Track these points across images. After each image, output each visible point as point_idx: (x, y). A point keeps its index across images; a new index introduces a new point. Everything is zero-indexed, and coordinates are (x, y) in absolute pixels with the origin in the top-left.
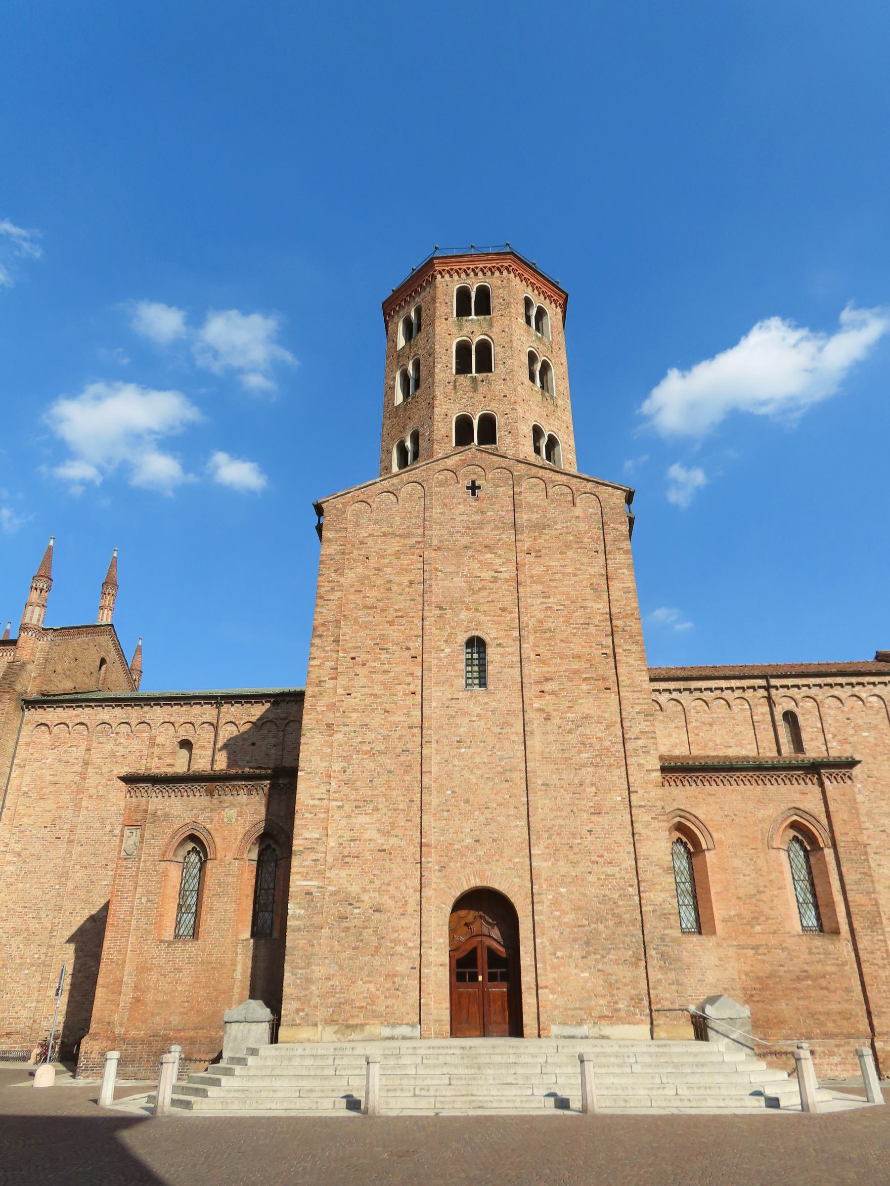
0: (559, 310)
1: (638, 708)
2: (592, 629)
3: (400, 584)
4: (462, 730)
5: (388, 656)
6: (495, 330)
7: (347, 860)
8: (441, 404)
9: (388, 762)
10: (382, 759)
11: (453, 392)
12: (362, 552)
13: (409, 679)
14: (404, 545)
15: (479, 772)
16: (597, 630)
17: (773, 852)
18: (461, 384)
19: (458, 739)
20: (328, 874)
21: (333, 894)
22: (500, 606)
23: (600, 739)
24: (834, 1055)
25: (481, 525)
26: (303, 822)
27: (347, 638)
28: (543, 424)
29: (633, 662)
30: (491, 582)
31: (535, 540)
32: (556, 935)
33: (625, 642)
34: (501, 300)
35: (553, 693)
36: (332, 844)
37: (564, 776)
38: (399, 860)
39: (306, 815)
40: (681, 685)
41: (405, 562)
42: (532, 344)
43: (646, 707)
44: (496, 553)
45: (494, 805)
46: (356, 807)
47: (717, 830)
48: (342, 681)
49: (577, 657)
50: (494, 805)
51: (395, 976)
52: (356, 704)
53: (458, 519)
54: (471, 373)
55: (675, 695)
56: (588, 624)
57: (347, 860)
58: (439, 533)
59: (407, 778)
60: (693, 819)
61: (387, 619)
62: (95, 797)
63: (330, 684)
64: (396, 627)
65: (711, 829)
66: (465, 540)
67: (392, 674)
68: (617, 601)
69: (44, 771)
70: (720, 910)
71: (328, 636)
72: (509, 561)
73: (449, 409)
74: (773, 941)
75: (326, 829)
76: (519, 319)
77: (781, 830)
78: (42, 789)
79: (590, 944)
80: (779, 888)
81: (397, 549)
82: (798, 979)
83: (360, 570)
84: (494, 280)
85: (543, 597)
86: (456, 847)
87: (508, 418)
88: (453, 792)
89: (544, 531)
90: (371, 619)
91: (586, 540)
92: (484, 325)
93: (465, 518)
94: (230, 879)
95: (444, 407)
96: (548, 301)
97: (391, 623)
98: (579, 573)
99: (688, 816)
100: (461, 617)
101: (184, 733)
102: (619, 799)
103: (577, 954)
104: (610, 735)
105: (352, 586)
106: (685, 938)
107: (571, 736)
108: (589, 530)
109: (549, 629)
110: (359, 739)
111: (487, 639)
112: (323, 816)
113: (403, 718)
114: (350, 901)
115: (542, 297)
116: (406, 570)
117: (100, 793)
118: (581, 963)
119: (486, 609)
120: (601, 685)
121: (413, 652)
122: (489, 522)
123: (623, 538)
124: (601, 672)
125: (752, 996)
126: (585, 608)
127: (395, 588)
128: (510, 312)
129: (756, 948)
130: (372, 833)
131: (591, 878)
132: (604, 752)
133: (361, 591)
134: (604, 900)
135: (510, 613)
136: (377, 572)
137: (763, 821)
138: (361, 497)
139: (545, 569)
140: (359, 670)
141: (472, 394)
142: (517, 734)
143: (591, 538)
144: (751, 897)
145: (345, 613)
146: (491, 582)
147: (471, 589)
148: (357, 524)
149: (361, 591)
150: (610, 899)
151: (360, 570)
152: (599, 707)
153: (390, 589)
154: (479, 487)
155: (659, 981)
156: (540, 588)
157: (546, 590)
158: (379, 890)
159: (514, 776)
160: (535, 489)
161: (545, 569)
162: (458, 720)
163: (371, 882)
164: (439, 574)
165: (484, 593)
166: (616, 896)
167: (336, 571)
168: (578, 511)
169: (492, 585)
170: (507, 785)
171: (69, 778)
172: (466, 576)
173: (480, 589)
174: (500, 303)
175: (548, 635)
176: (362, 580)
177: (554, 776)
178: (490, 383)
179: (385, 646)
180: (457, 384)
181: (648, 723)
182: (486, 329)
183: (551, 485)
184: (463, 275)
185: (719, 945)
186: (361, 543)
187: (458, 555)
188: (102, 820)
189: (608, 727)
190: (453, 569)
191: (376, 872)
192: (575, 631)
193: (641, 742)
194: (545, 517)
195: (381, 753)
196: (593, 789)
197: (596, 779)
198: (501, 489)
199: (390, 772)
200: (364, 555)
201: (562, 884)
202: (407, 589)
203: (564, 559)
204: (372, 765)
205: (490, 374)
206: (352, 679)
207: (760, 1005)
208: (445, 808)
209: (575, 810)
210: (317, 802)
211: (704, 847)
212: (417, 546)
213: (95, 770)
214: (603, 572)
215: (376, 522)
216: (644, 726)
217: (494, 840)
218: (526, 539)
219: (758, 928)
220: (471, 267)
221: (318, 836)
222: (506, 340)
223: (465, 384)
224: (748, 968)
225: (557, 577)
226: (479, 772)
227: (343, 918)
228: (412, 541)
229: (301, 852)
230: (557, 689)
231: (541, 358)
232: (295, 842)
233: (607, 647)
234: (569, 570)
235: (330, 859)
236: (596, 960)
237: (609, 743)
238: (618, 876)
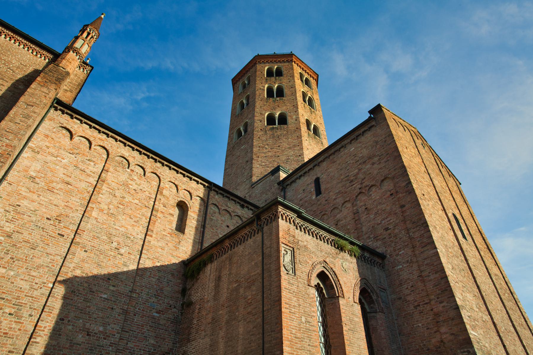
62: (105, 212)
69: (58, 167)
78: (52, 182)
101: (183, 196)
117: (111, 211)
171: (83, 185)
188: (110, 235)
213: (109, 190)
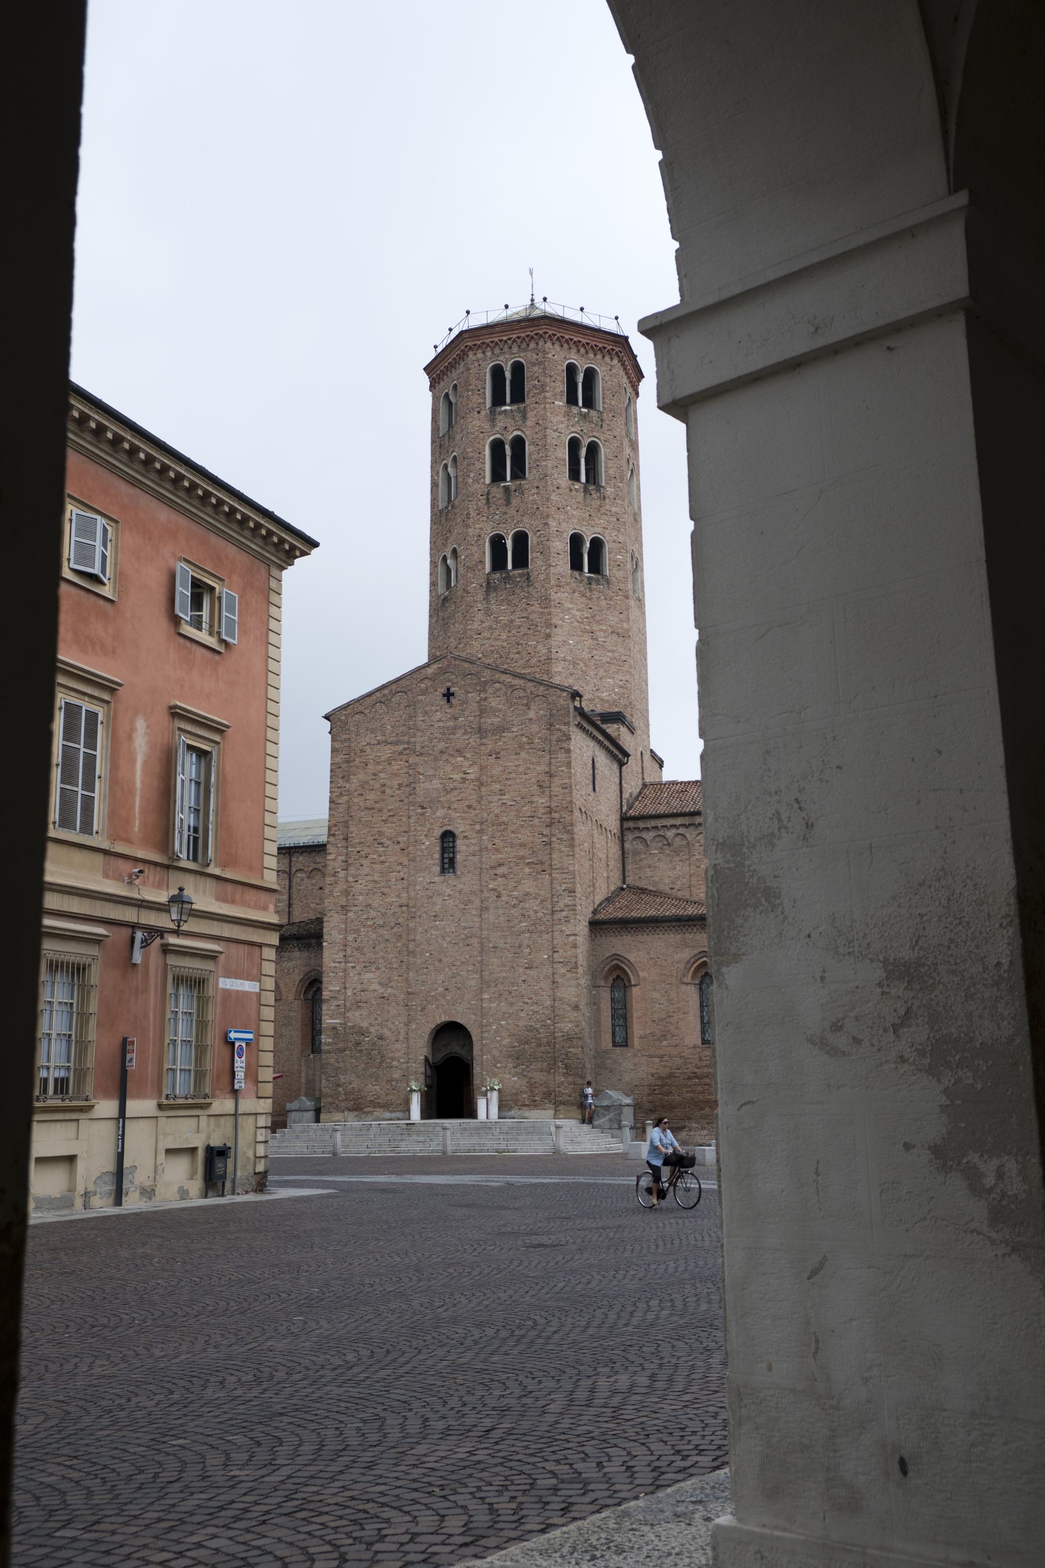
0: (615, 361)
1: (564, 887)
2: (536, 821)
3: (391, 788)
4: (438, 908)
5: (383, 849)
6: (529, 423)
7: (359, 1004)
8: (474, 523)
10: (381, 931)
11: (486, 507)
12: (362, 760)
13: (399, 868)
14: (395, 752)
15: (449, 939)
16: (540, 822)
17: (683, 987)
18: (494, 497)
19: (434, 914)
20: (347, 1015)
21: (351, 1027)
22: (467, 804)
23: (536, 912)
24: (705, 1128)
26: (328, 979)
27: (354, 835)
28: (584, 529)
29: (563, 849)
31: (496, 743)
32: (496, 1053)
33: (560, 832)
34: (536, 382)
35: (504, 876)
36: (349, 994)
37: (509, 941)
38: (394, 1004)
39: (331, 974)
40: (686, 820)
41: (395, 768)
42: (573, 430)
43: (570, 885)
44: (464, 757)
45: (459, 963)
46: (364, 967)
47: (643, 970)
48: (352, 870)
49: (523, 845)
50: (459, 963)
51: (392, 1081)
52: (362, 889)
53: (437, 725)
54: (504, 479)
55: (681, 830)
56: (533, 817)
57: (359, 1004)
58: (421, 739)
59: (399, 944)
60: (627, 962)
63: (342, 874)
64: (389, 825)
65: (638, 969)
66: (441, 745)
67: (387, 864)
68: (556, 796)
70: (638, 1030)
71: (339, 835)
72: (475, 763)
73: (481, 529)
74: (675, 1052)
75: (344, 983)
76: (557, 403)
77: (692, 969)
79: (519, 1058)
80: (684, 1013)
82: (689, 1078)
83: (361, 776)
84: (529, 354)
85: (501, 795)
86: (432, 994)
87: (539, 537)
88: (431, 954)
89: (504, 734)
90: (370, 819)
91: (537, 741)
92: (518, 416)
93: (441, 724)
94: (292, 1014)
95: (477, 526)
96: (599, 357)
97: (385, 821)
98: (529, 772)
99: (622, 959)
100: (438, 814)
102: (546, 956)
103: (510, 1065)
104: (543, 908)
105: (356, 790)
106: (618, 1050)
107: (515, 910)
108: (540, 732)
109: (504, 822)
110: (365, 916)
111: (457, 832)
112: (341, 974)
114: (363, 1032)
115: (591, 355)
116: (396, 775)
118: (513, 1071)
119: (456, 806)
120: (539, 867)
121: (402, 845)
122: (460, 728)
123: (565, 738)
124: (540, 858)
125: (654, 1090)
126: (531, 802)
127: (388, 791)
128: (545, 398)
129: (661, 1057)
130: (375, 986)
131: (522, 1014)
132: (538, 921)
133: (362, 795)
134: (530, 1028)
135: (475, 809)
137: (679, 962)
138: (360, 708)
139: (502, 768)
140: (363, 861)
141: (503, 509)
142: (476, 909)
143: (540, 738)
144: (662, 1020)
145: (352, 814)
147: (445, 790)
148: (357, 735)
149: (362, 795)
150: (535, 1028)
151: (361, 776)
152: (537, 886)
153: (384, 792)
154: (453, 694)
155: (562, 1083)
156: (498, 786)
157: (502, 788)
158: (381, 1025)
159: (472, 941)
160: (498, 693)
161: (502, 768)
162: (435, 900)
163: (376, 1019)
164: (421, 777)
165: (455, 793)
166: (538, 1026)
167: (343, 777)
168: (532, 714)
169: (461, 786)
170: (468, 948)
172: (442, 778)
173: (452, 789)
174: (534, 386)
175: (502, 828)
176: (363, 784)
177: (501, 941)
178: (522, 493)
180: (490, 496)
181: (571, 898)
182: (520, 423)
183: (511, 690)
184: (497, 351)
185: (635, 1055)
187: (436, 759)
189: (542, 902)
190: (431, 772)
191: (379, 1013)
193: (564, 914)
194: (504, 720)
195: (381, 926)
196: (528, 950)
197: (531, 942)
198: (470, 695)
199: (387, 940)
201: (503, 1019)
202: (397, 792)
203: (517, 760)
205: (523, 482)
206: (358, 869)
207: (659, 1096)
208: (425, 966)
209: (515, 965)
210: (337, 965)
211: (633, 983)
212: (405, 752)
216: (568, 900)
217: (458, 989)
218: (489, 742)
219: (665, 1043)
220: (505, 338)
221: (338, 989)
222: (540, 435)
223: (498, 496)
224: (653, 1071)
225: (511, 776)
227: (358, 1044)
228: (401, 747)
229: (328, 1000)
230: (506, 872)
231: (585, 442)
232: (324, 993)
233: (546, 836)
234: (521, 769)
235: (348, 1004)
236: (523, 1070)
237: (542, 914)
238: (541, 1012)
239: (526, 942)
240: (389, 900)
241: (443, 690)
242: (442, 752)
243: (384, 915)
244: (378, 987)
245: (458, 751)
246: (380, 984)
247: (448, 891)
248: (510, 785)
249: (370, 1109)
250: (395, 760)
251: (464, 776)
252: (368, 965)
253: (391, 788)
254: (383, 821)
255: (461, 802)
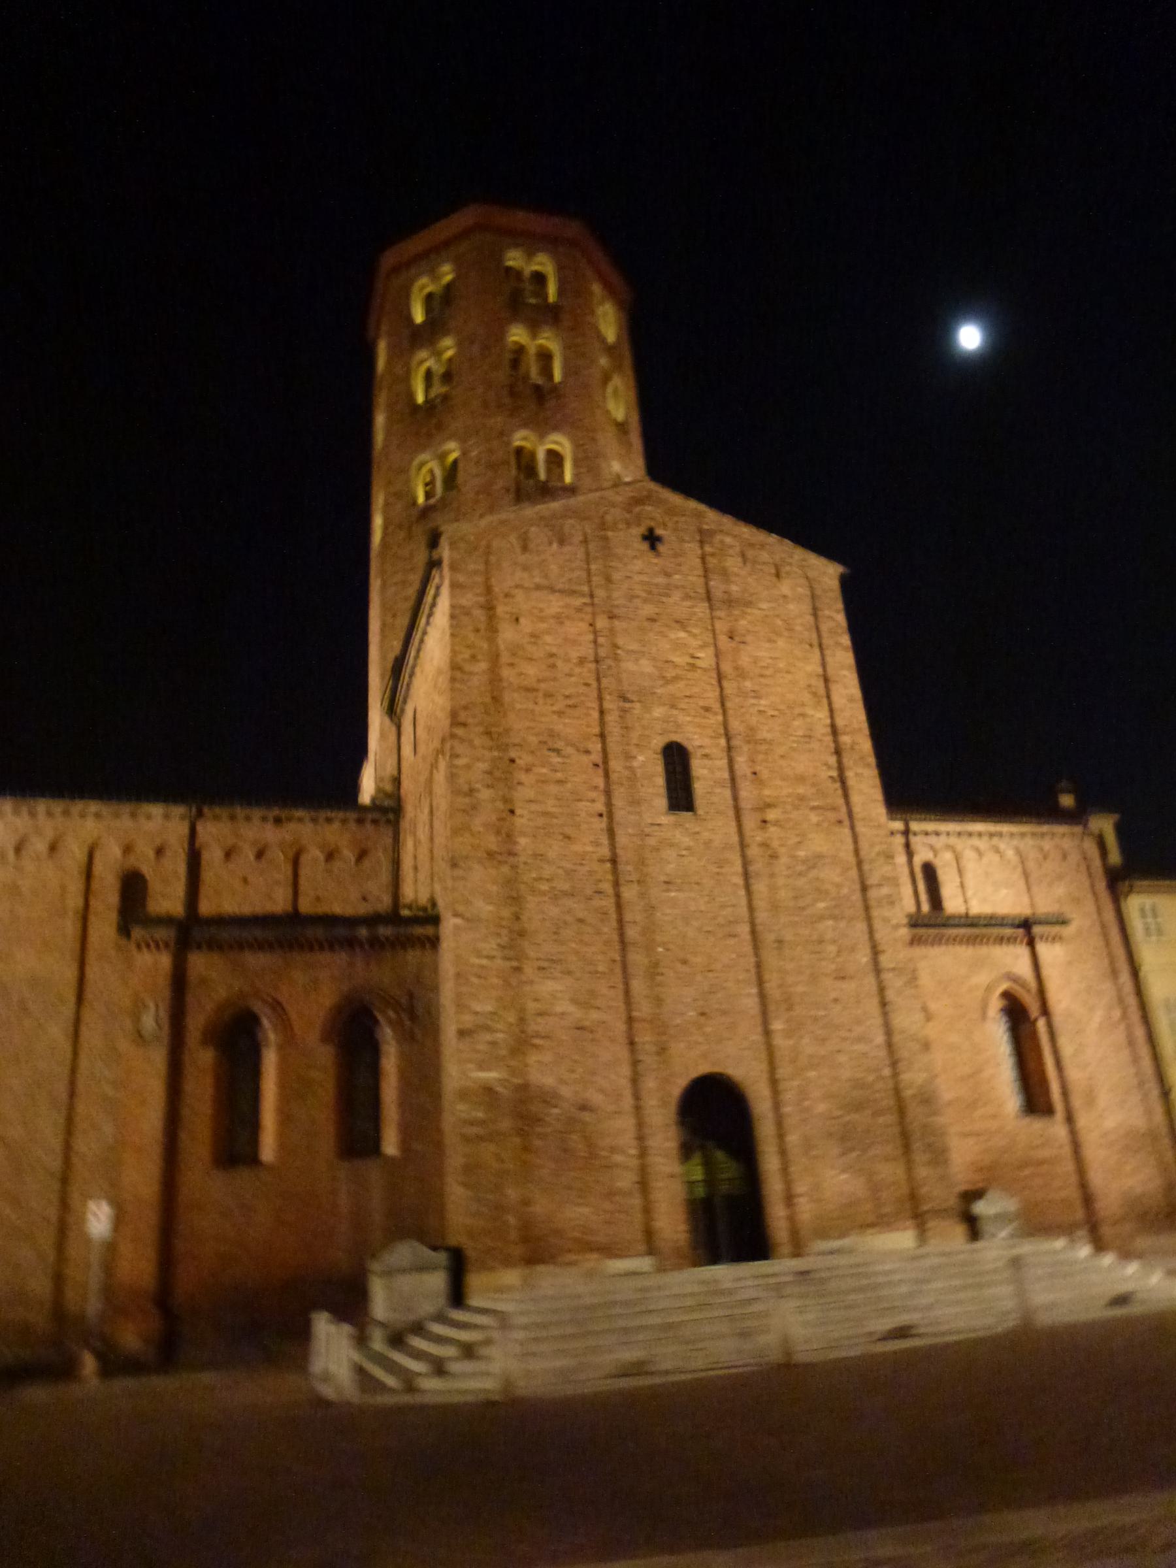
1: (877, 848)
2: (815, 745)
5: (559, 760)
9: (578, 908)
10: (569, 902)
13: (593, 795)
14: (567, 606)
15: (695, 924)
19: (663, 878)
22: (701, 703)
25: (667, 590)
30: (686, 670)
35: (777, 823)
49: (801, 779)
53: (637, 578)
61: (555, 708)
66: (649, 610)
67: (569, 786)
79: (847, 1138)
81: (559, 610)
90: (531, 706)
97: (560, 713)
113: (589, 849)
116: (574, 642)
120: (832, 816)
122: (677, 587)
126: (803, 715)
127: (559, 663)
131: (842, 1058)
134: (858, 1084)
136: (533, 640)
140: (523, 777)
143: (802, 625)
146: (686, 670)
153: (553, 666)
157: (756, 688)
165: (681, 684)
170: (732, 941)
179: (556, 746)
186: (507, 595)
190: (634, 646)
192: (795, 745)
195: (565, 894)
198: (687, 545)
199: (581, 921)
200: (512, 614)
202: (577, 670)
204: (554, 911)
210: (484, 962)
214: (820, 670)
215: (526, 568)
225: (768, 672)
226: (695, 924)
239: (829, 935)
240: (577, 848)
241: (642, 530)
242: (652, 620)
243: (569, 873)
244: (571, 1008)
245: (677, 622)
246: (574, 1001)
247: (687, 841)
248: (767, 685)
249: (572, 1257)
250: (568, 617)
251: (691, 661)
252: (546, 964)
253: (567, 660)
254: (554, 712)
255: (691, 701)
